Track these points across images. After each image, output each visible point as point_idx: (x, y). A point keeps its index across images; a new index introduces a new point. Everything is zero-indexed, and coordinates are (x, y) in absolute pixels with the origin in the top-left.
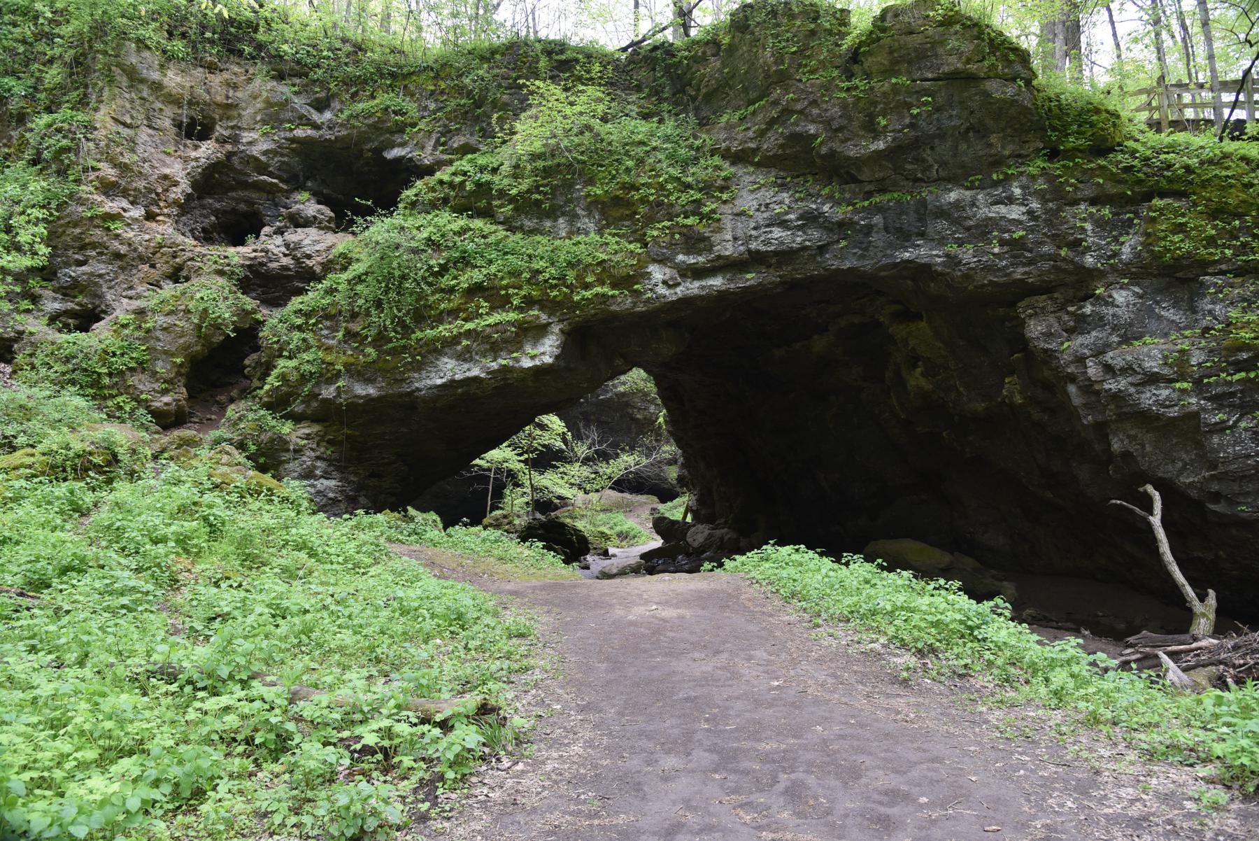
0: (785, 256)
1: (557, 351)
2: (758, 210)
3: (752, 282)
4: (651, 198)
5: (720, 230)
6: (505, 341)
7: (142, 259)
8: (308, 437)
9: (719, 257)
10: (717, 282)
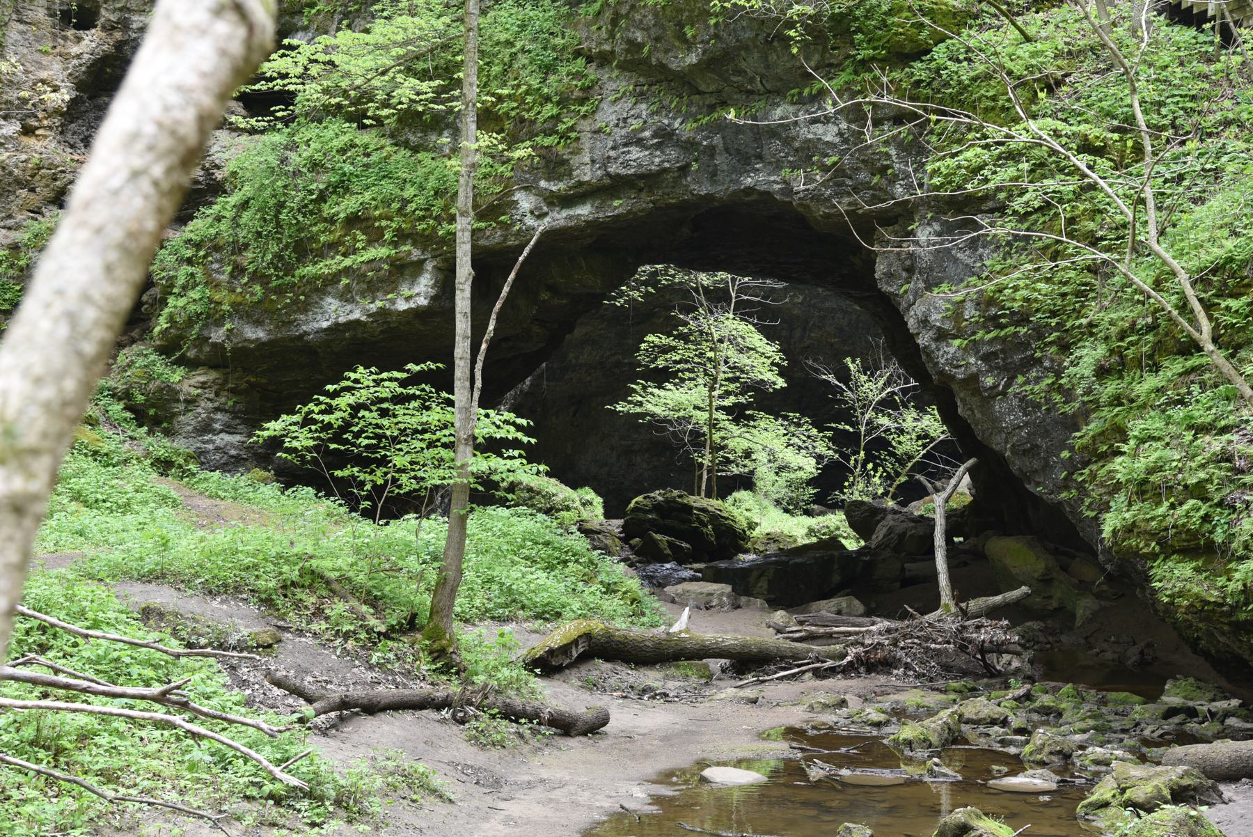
1: (432, 292)
2: (617, 126)
3: (620, 210)
4: (513, 114)
6: (381, 281)
7: (19, 183)
8: (203, 385)
9: (580, 183)
10: (584, 211)
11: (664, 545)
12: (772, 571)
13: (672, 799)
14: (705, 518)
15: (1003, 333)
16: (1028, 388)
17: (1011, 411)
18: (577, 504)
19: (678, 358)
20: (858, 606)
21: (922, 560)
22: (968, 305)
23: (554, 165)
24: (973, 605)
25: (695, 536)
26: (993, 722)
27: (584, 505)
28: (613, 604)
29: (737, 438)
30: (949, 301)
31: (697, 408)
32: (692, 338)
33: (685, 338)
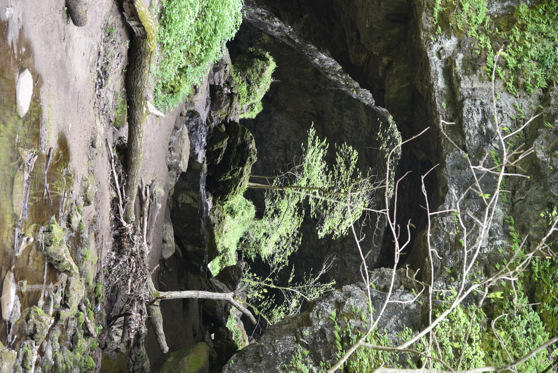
0: (458, 129)
2: (497, 106)
3: (438, 107)
4: (511, 38)
5: (481, 79)
9: (459, 81)
10: (440, 83)
11: (220, 146)
12: (197, 206)
13: (5, 39)
14: (236, 174)
15: (338, 342)
16: (300, 356)
17: (285, 345)
18: (252, 101)
19: (342, 171)
20: (168, 255)
21: (200, 309)
22: (359, 322)
23: (473, 64)
24: (157, 311)
25: (225, 167)
26: (65, 298)
27: (251, 105)
28: (171, 72)
29: (287, 206)
30: (362, 310)
31: (309, 180)
32: (354, 180)
33: (354, 176)
